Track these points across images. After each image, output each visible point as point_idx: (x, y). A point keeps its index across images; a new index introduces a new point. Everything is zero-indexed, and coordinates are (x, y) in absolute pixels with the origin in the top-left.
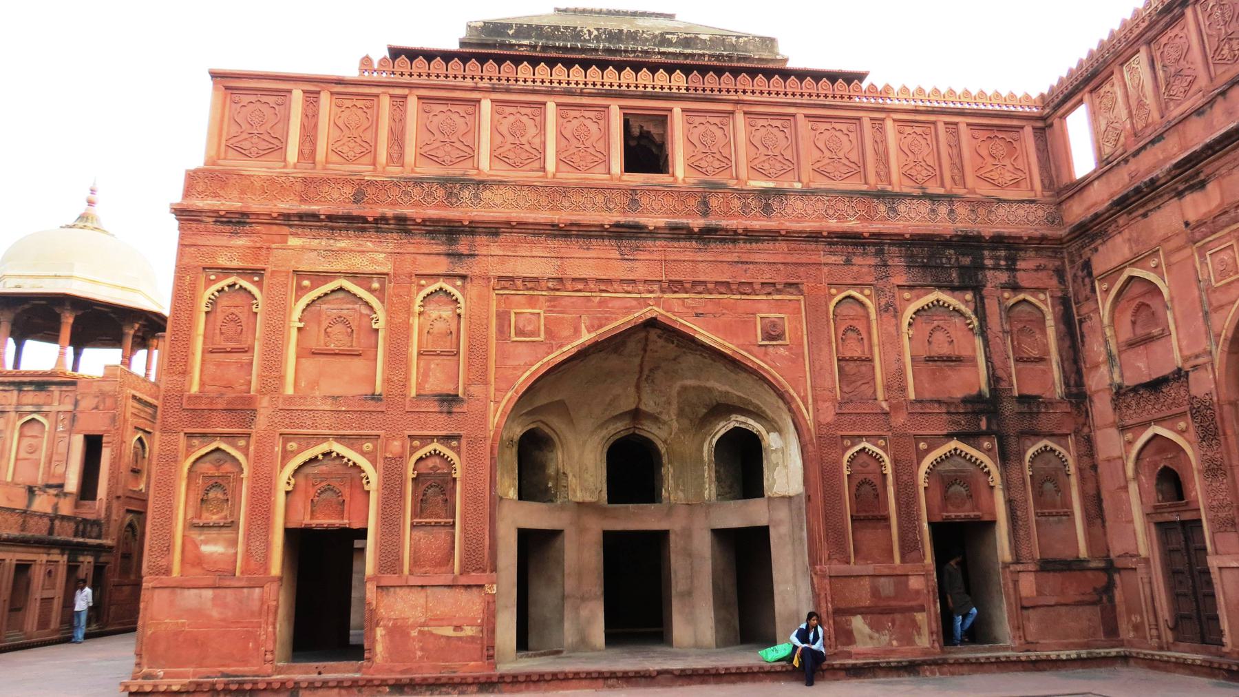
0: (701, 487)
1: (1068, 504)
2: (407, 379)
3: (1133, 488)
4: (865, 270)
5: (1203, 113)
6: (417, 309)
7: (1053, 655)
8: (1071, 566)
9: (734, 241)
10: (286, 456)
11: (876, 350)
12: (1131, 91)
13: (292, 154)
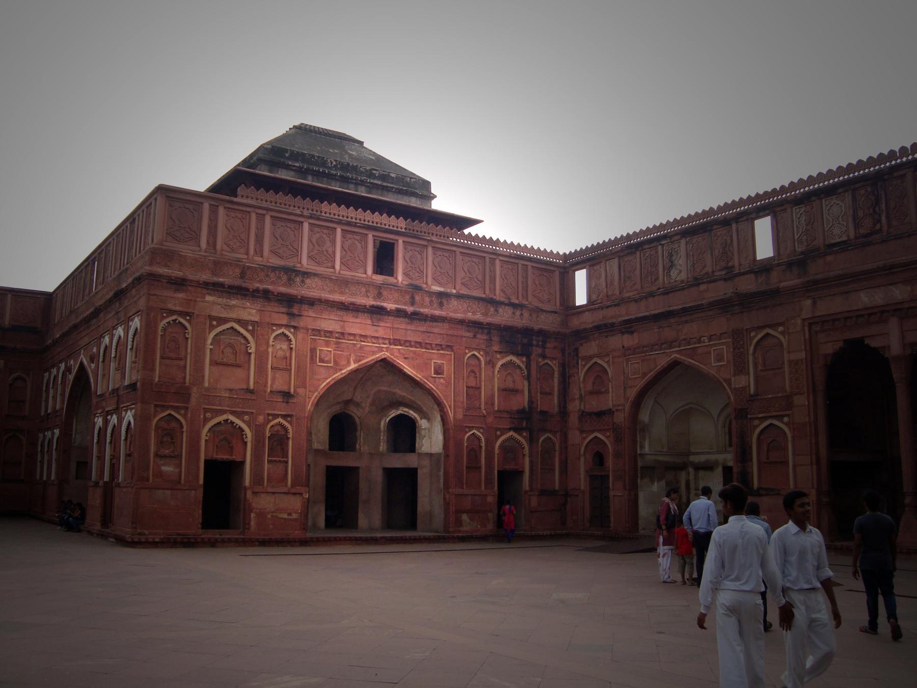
0: (378, 445)
2: (267, 383)
3: (582, 459)
6: (271, 343)
7: (541, 533)
9: (425, 320)
10: (206, 420)
11: (483, 383)
12: (609, 275)
13: (204, 244)
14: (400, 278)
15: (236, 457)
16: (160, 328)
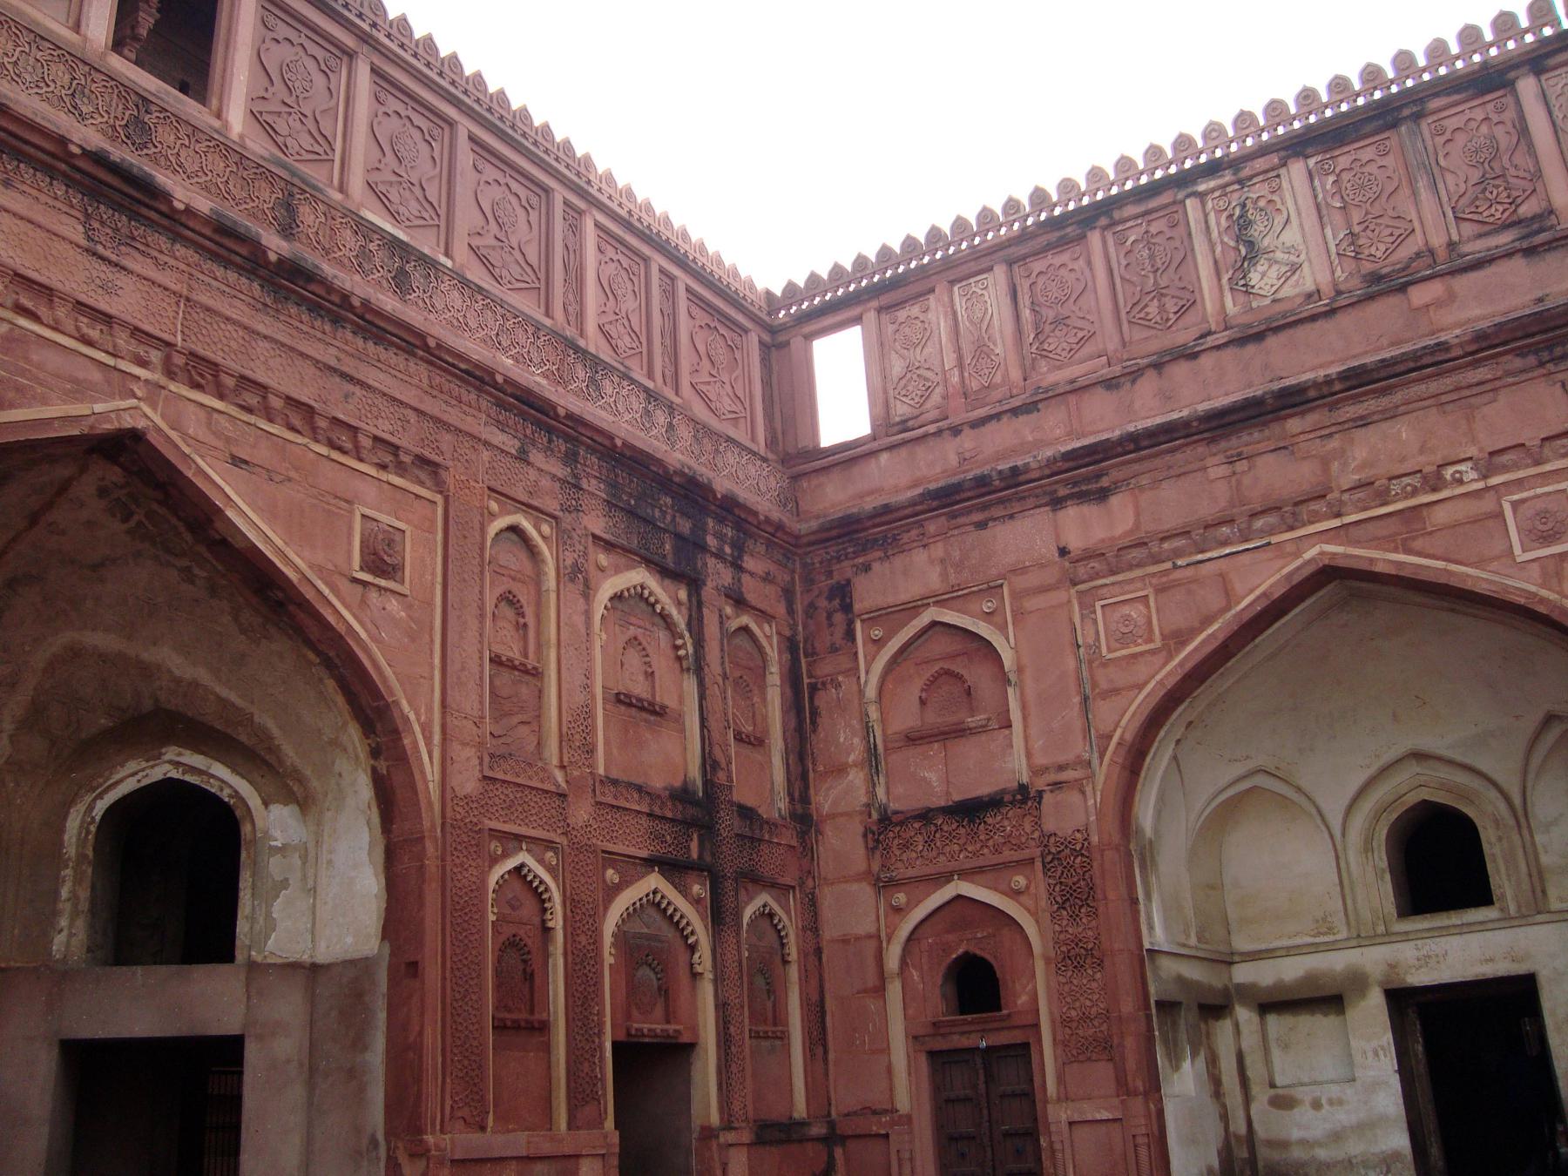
0: (46, 921)
1: (779, 1017)
4: (545, 483)
5: (1117, 386)
9: (337, 320)
12: (964, 324)
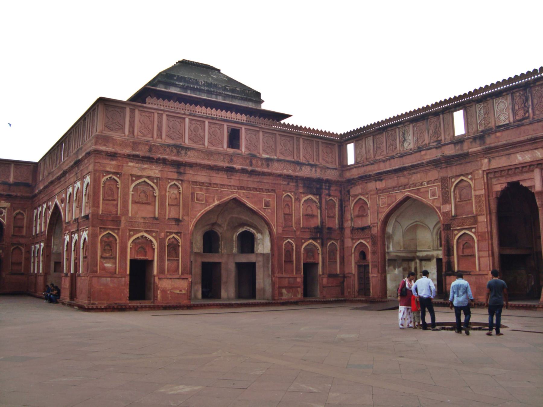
0: (232, 249)
1: (336, 259)
2: (166, 213)
6: (168, 190)
7: (329, 299)
8: (335, 276)
9: (259, 175)
10: (130, 236)
13: (127, 133)
14: (243, 149)
15: (149, 258)
16: (102, 183)
